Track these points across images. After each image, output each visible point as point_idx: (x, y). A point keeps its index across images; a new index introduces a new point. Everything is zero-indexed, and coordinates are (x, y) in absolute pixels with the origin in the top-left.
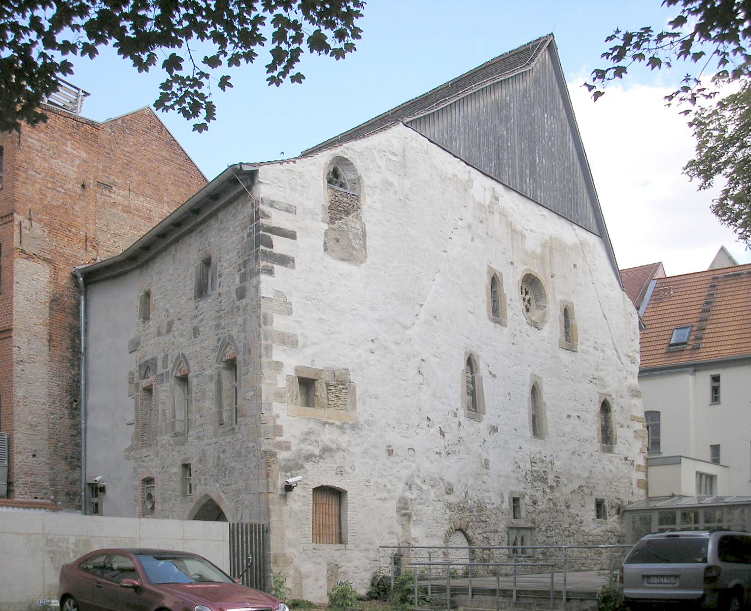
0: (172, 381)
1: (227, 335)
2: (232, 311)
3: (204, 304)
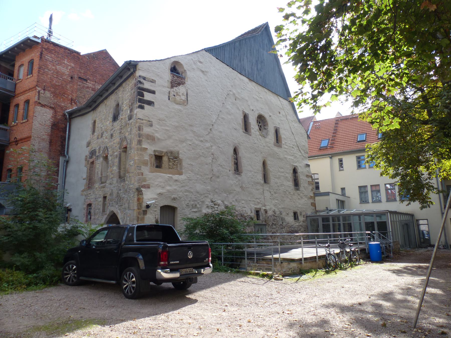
0: (101, 159)
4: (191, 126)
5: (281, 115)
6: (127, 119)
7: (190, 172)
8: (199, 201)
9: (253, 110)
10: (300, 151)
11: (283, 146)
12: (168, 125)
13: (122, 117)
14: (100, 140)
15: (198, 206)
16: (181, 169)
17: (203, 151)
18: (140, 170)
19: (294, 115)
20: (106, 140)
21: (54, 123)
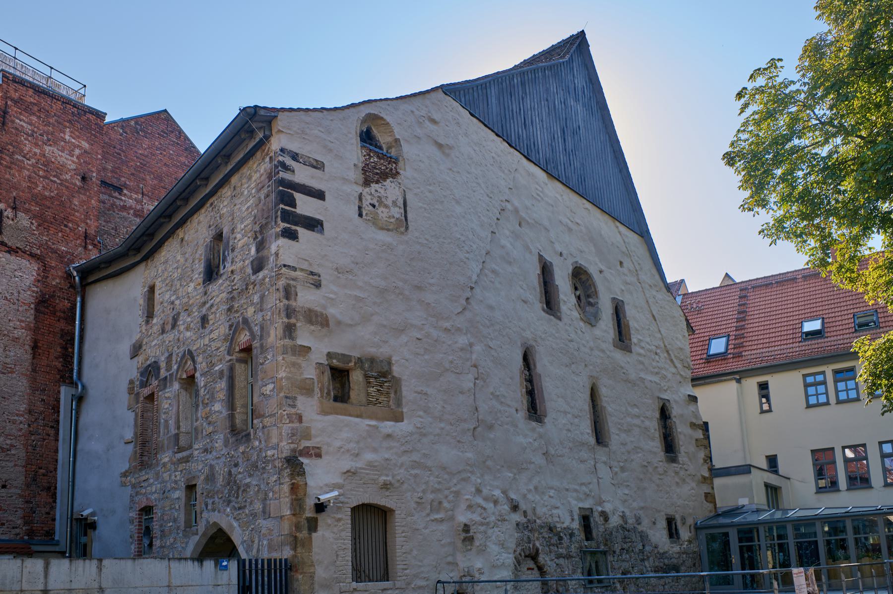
1: (241, 319)
2: (247, 289)
3: (214, 288)
4: (419, 288)
5: (625, 270)
6: (249, 270)
7: (421, 413)
8: (447, 492)
9: (561, 254)
10: (672, 361)
11: (634, 348)
12: (360, 284)
13: (234, 267)
14: (170, 337)
15: (446, 505)
16: (399, 403)
17: (450, 358)
18: (294, 406)
19: (654, 271)
20: (187, 333)
21: (43, 295)
